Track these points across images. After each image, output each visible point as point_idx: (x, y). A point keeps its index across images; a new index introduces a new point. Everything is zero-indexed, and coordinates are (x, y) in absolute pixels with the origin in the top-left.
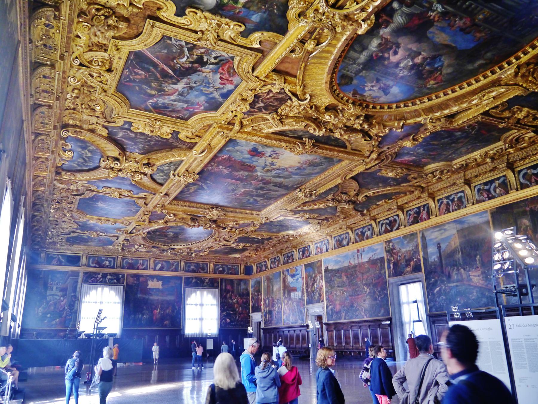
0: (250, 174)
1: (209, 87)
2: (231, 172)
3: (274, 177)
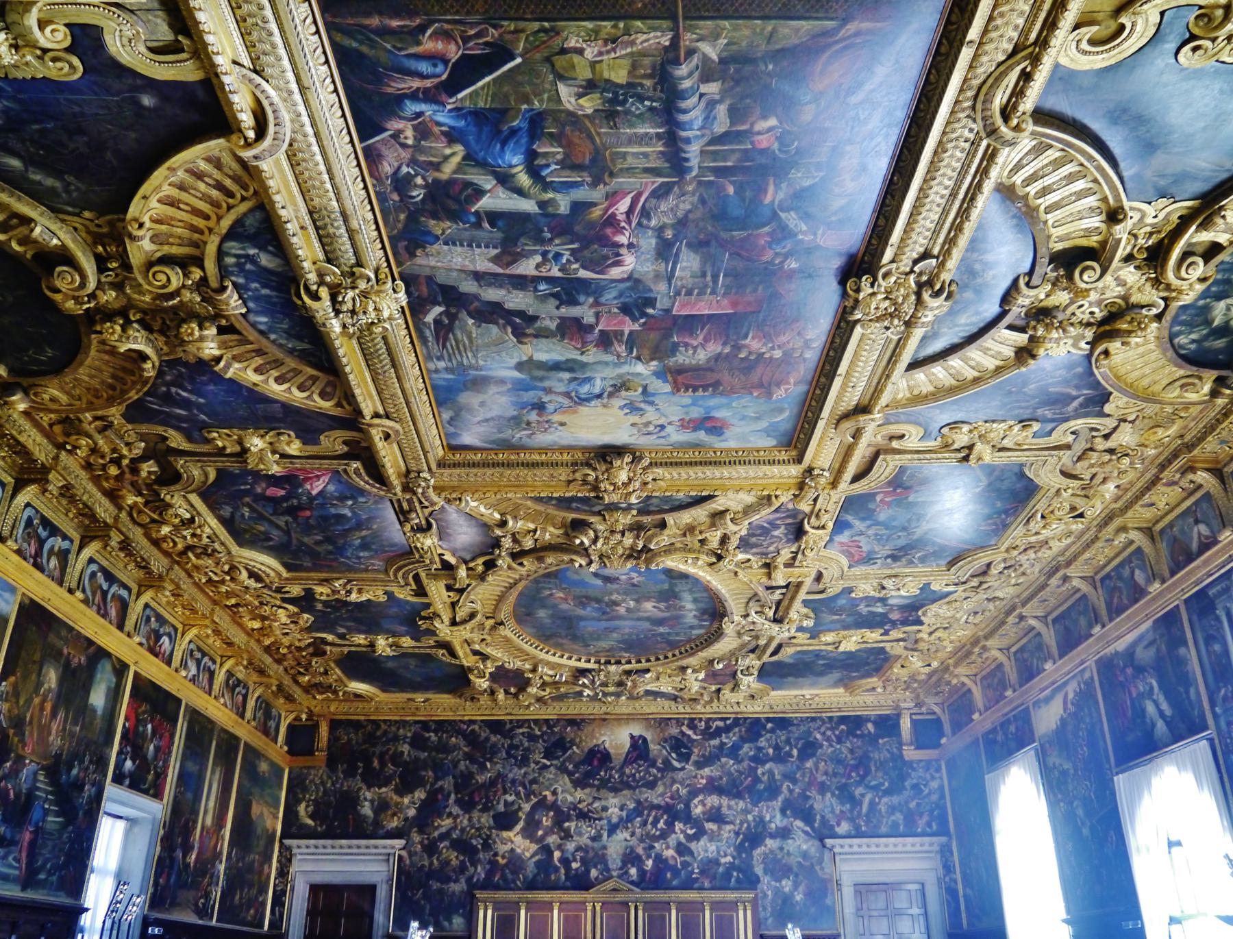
0: (671, 362)
1: (876, 535)
2: (737, 348)
3: (584, 365)
